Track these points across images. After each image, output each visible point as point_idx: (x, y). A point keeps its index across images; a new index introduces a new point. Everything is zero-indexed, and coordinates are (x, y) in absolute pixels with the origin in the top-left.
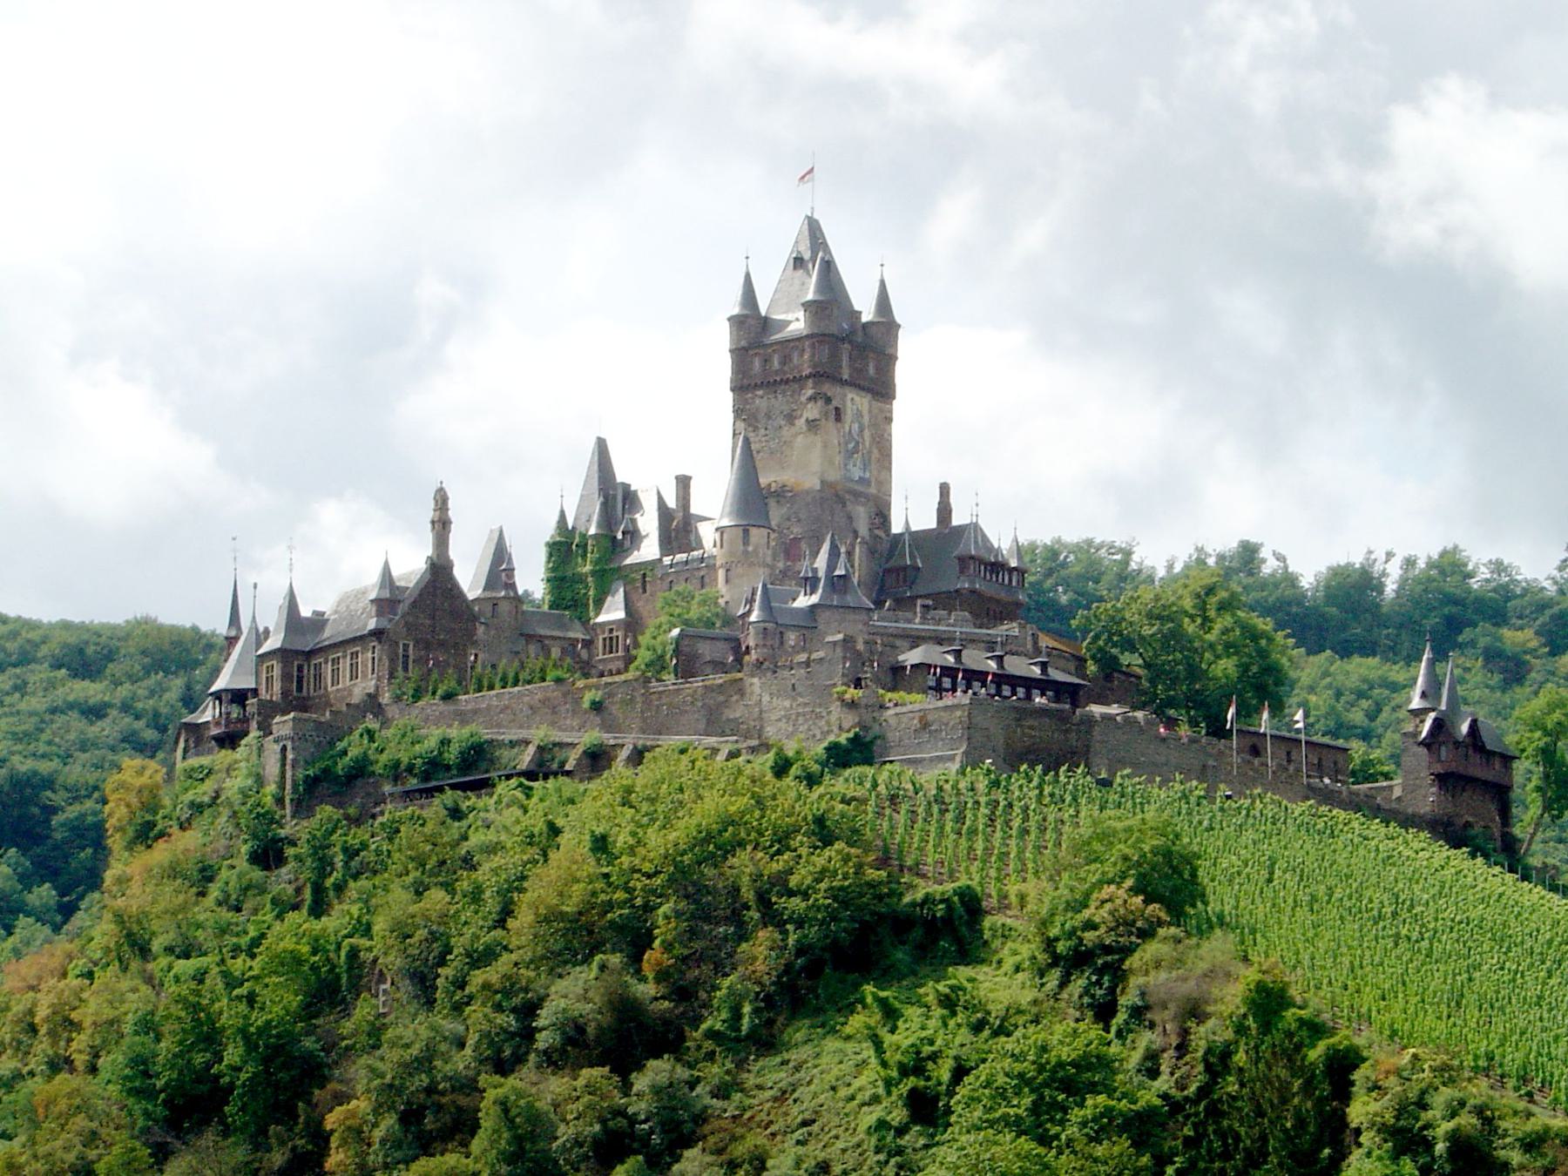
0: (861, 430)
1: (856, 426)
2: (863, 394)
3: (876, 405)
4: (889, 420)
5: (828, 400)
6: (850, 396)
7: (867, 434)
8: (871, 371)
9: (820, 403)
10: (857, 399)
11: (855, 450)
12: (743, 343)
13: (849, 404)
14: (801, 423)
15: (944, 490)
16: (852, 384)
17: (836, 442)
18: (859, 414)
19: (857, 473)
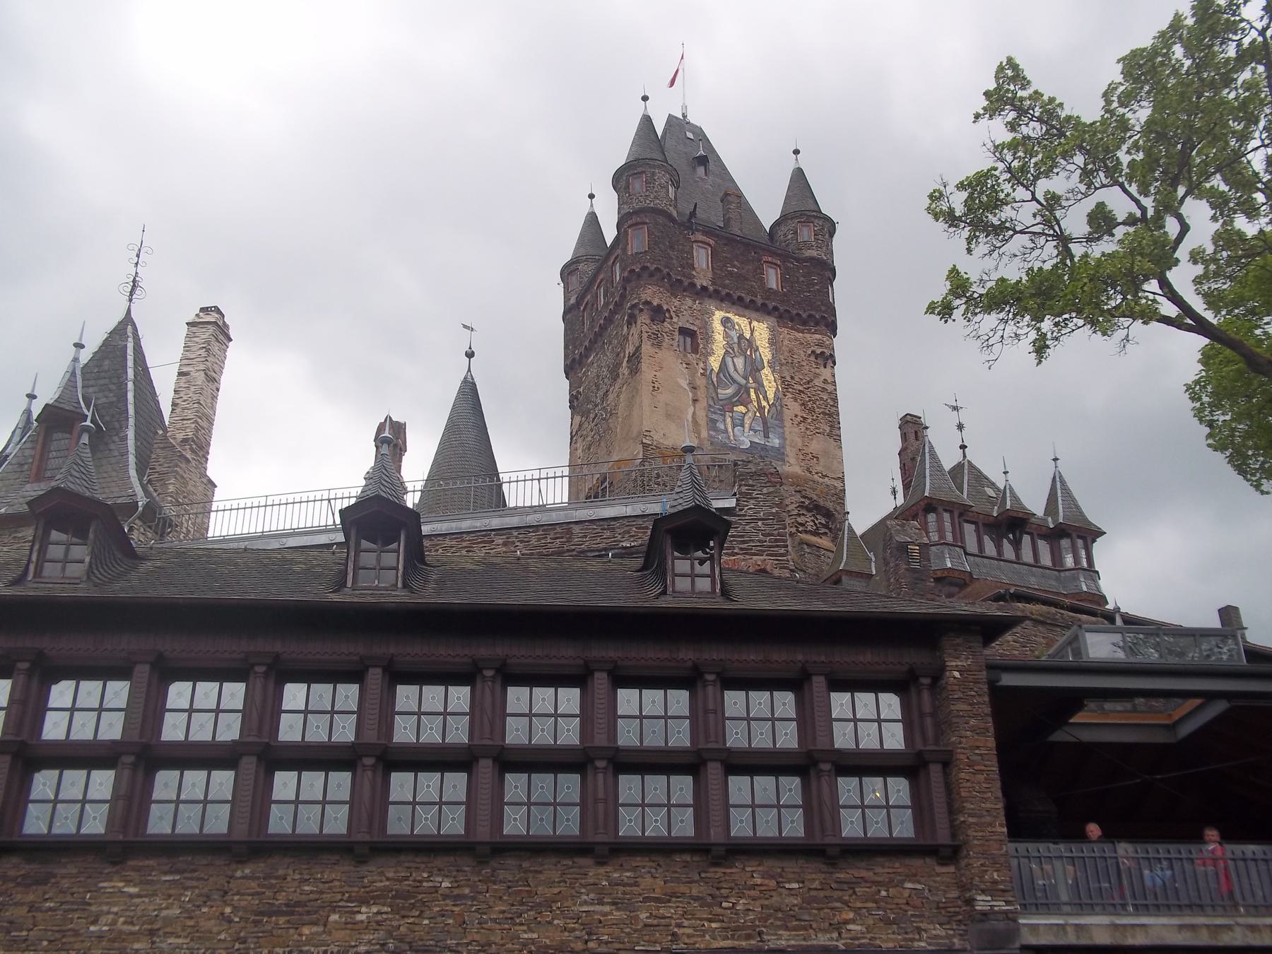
0: (754, 368)
1: (740, 362)
2: (754, 315)
4: (828, 359)
5: (658, 314)
6: (719, 315)
7: (767, 376)
8: (772, 279)
9: (643, 318)
10: (736, 319)
11: (741, 396)
12: (573, 301)
14: (624, 370)
15: (912, 428)
17: (684, 384)
18: (744, 345)
19: (746, 438)
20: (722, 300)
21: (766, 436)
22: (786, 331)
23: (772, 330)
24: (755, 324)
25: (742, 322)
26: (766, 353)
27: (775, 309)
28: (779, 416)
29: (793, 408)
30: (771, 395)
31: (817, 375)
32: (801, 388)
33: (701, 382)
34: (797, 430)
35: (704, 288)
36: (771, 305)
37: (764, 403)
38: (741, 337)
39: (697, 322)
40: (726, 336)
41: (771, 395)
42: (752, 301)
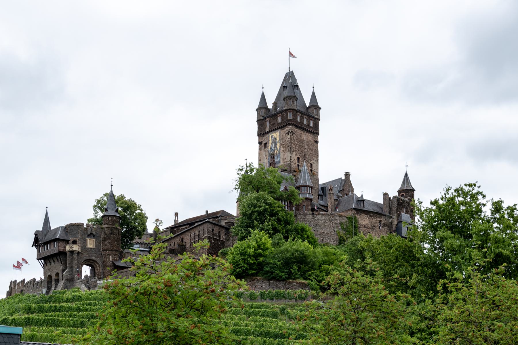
1: (273, 145)
2: (275, 132)
3: (282, 132)
7: (278, 145)
13: (270, 138)
16: (271, 131)
17: (264, 156)
20: (271, 132)
21: (277, 159)
22: (282, 131)
23: (280, 133)
24: (277, 133)
25: (274, 134)
26: (278, 139)
27: (280, 127)
28: (279, 154)
29: (282, 149)
30: (278, 149)
31: (287, 138)
32: (284, 143)
33: (267, 153)
34: (282, 154)
35: (268, 132)
36: (278, 127)
37: (277, 152)
38: (274, 138)
39: (267, 140)
40: (272, 139)
41: (278, 149)
42: (276, 128)
